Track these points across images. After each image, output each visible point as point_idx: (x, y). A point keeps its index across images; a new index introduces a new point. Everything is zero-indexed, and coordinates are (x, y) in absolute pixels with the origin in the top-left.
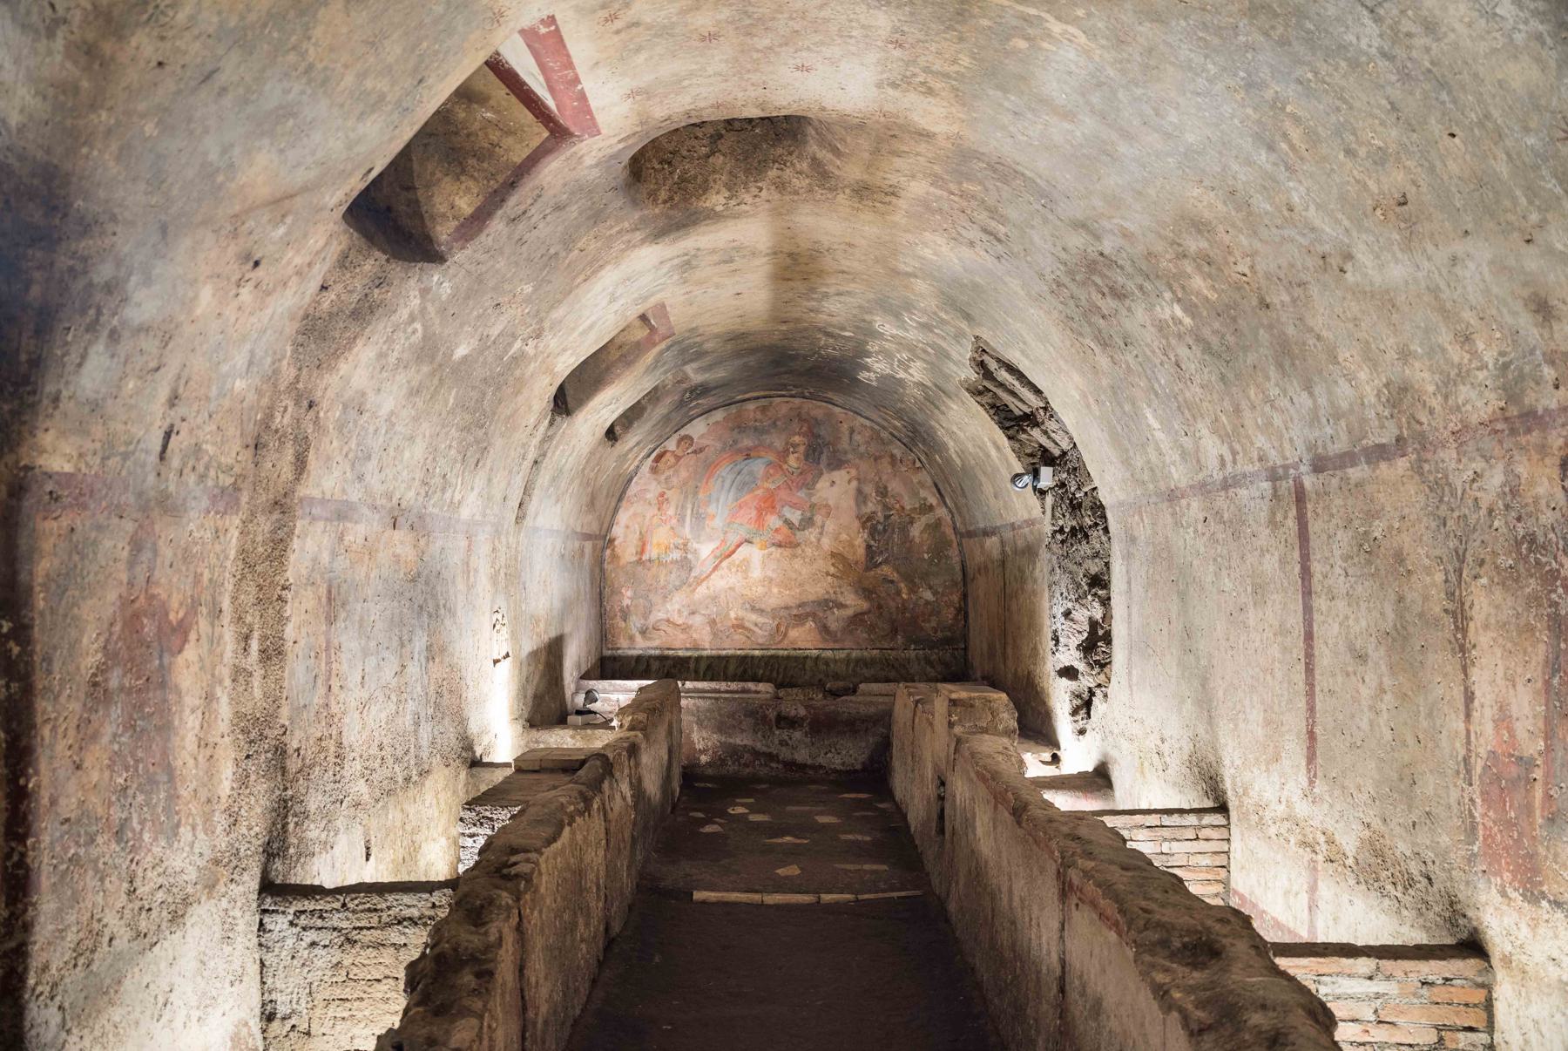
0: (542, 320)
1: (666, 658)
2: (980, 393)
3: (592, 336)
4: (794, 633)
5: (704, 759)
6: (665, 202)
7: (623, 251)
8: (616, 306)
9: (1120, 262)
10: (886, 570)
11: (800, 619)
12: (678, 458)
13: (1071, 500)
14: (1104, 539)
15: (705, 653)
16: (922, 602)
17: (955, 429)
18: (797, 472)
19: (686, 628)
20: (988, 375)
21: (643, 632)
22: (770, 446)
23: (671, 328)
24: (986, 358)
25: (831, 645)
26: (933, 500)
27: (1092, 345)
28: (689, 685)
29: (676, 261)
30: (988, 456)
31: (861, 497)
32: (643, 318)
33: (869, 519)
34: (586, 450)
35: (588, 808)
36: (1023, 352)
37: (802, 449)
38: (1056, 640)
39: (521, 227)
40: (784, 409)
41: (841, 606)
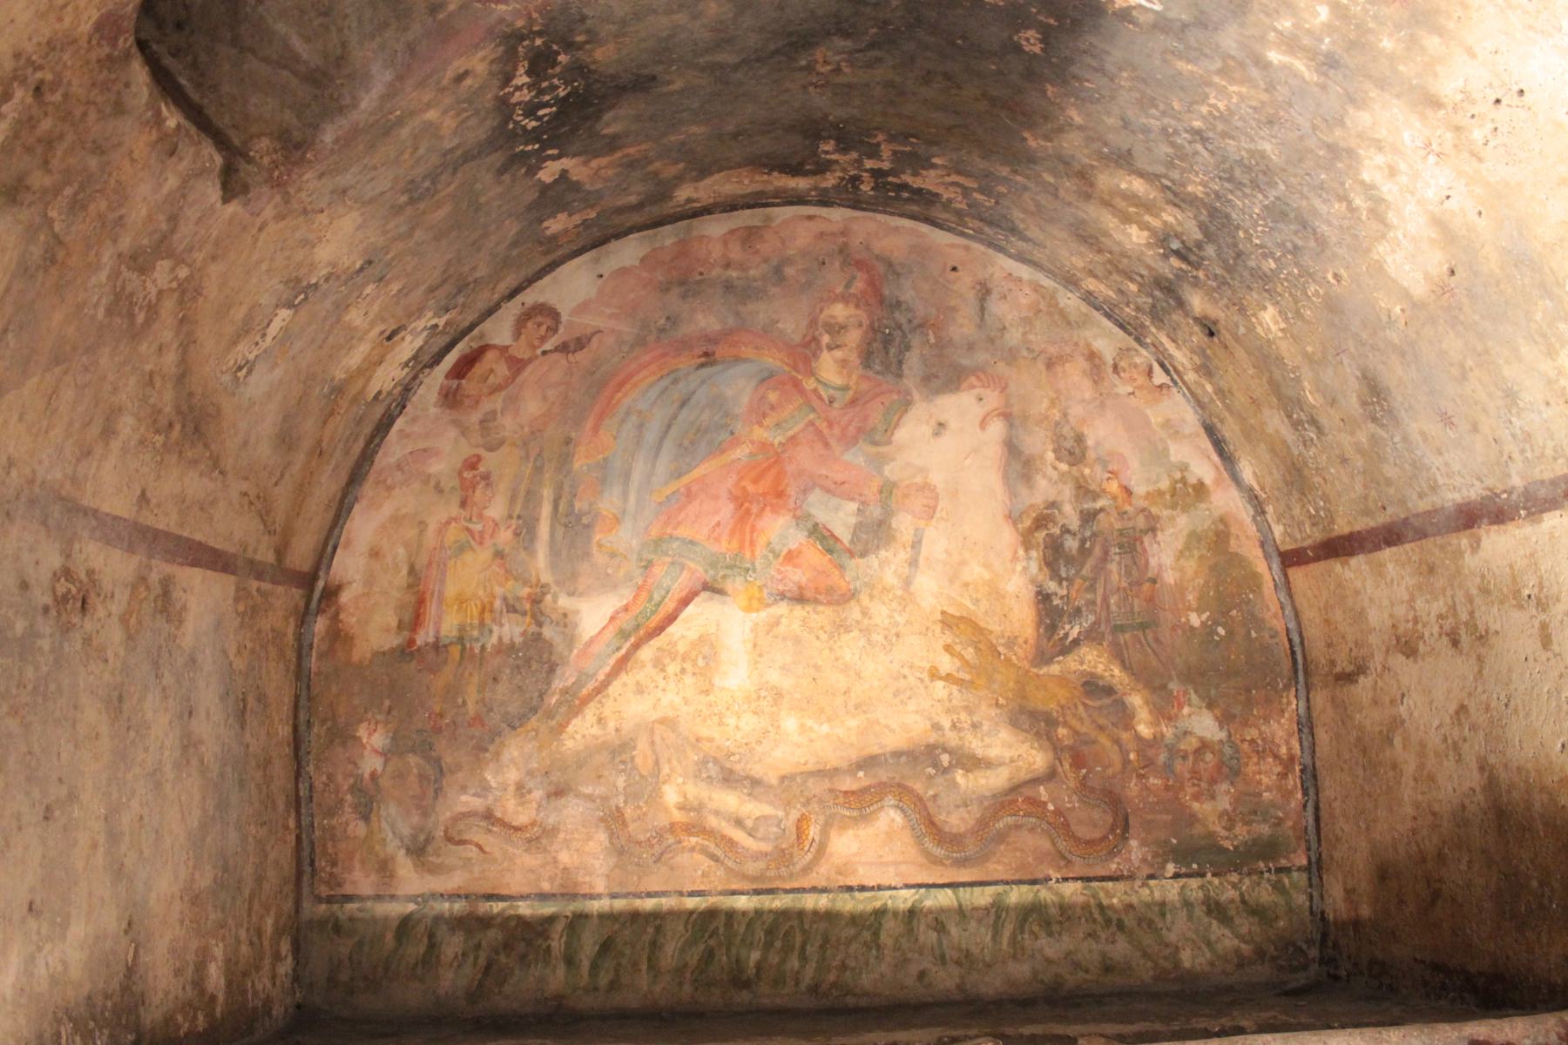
1: (486, 922)
10: (1092, 660)
11: (861, 803)
12: (517, 365)
15: (596, 906)
19: (538, 837)
21: (419, 850)
33: (1041, 522)
37: (854, 337)
41: (973, 763)
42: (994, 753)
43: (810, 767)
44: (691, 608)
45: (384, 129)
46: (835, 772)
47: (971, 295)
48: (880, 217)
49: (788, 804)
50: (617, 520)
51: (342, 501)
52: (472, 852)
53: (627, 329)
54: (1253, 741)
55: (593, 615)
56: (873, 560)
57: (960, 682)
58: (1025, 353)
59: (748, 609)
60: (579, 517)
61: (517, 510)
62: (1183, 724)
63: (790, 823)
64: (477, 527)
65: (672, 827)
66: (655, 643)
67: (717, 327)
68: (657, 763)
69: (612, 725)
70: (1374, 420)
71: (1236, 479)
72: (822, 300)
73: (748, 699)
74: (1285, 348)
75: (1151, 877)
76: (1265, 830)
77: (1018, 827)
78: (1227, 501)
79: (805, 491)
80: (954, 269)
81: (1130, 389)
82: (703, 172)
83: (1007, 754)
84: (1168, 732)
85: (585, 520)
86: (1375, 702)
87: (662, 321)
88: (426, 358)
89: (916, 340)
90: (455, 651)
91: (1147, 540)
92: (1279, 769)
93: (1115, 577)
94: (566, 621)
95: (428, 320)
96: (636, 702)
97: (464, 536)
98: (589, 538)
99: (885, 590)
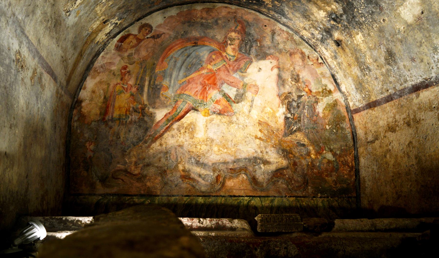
10: (299, 136)
12: (139, 41)
16: (325, 161)
18: (233, 59)
19: (141, 178)
21: (104, 180)
22: (213, 39)
25: (259, 194)
31: (281, 81)
33: (286, 97)
37: (237, 42)
40: (224, 13)
41: (266, 162)
42: (271, 160)
44: (188, 115)
48: (246, 9)
49: (214, 171)
50: (168, 88)
51: (84, 75)
52: (120, 182)
53: (172, 34)
54: (342, 161)
55: (160, 114)
56: (240, 104)
58: (284, 51)
59: (205, 116)
60: (156, 87)
61: (138, 82)
62: (324, 156)
64: (126, 87)
66: (178, 123)
67: (199, 36)
68: (177, 157)
69: (164, 146)
70: (389, 64)
71: (340, 90)
72: (228, 31)
73: (204, 141)
75: (314, 197)
79: (222, 84)
80: (266, 26)
81: (312, 63)
83: (276, 161)
85: (158, 87)
86: (380, 147)
87: (183, 32)
88: (112, 35)
89: (254, 45)
92: (349, 170)
93: (306, 114)
94: (152, 116)
96: (170, 140)
97: (121, 89)
98: (159, 92)
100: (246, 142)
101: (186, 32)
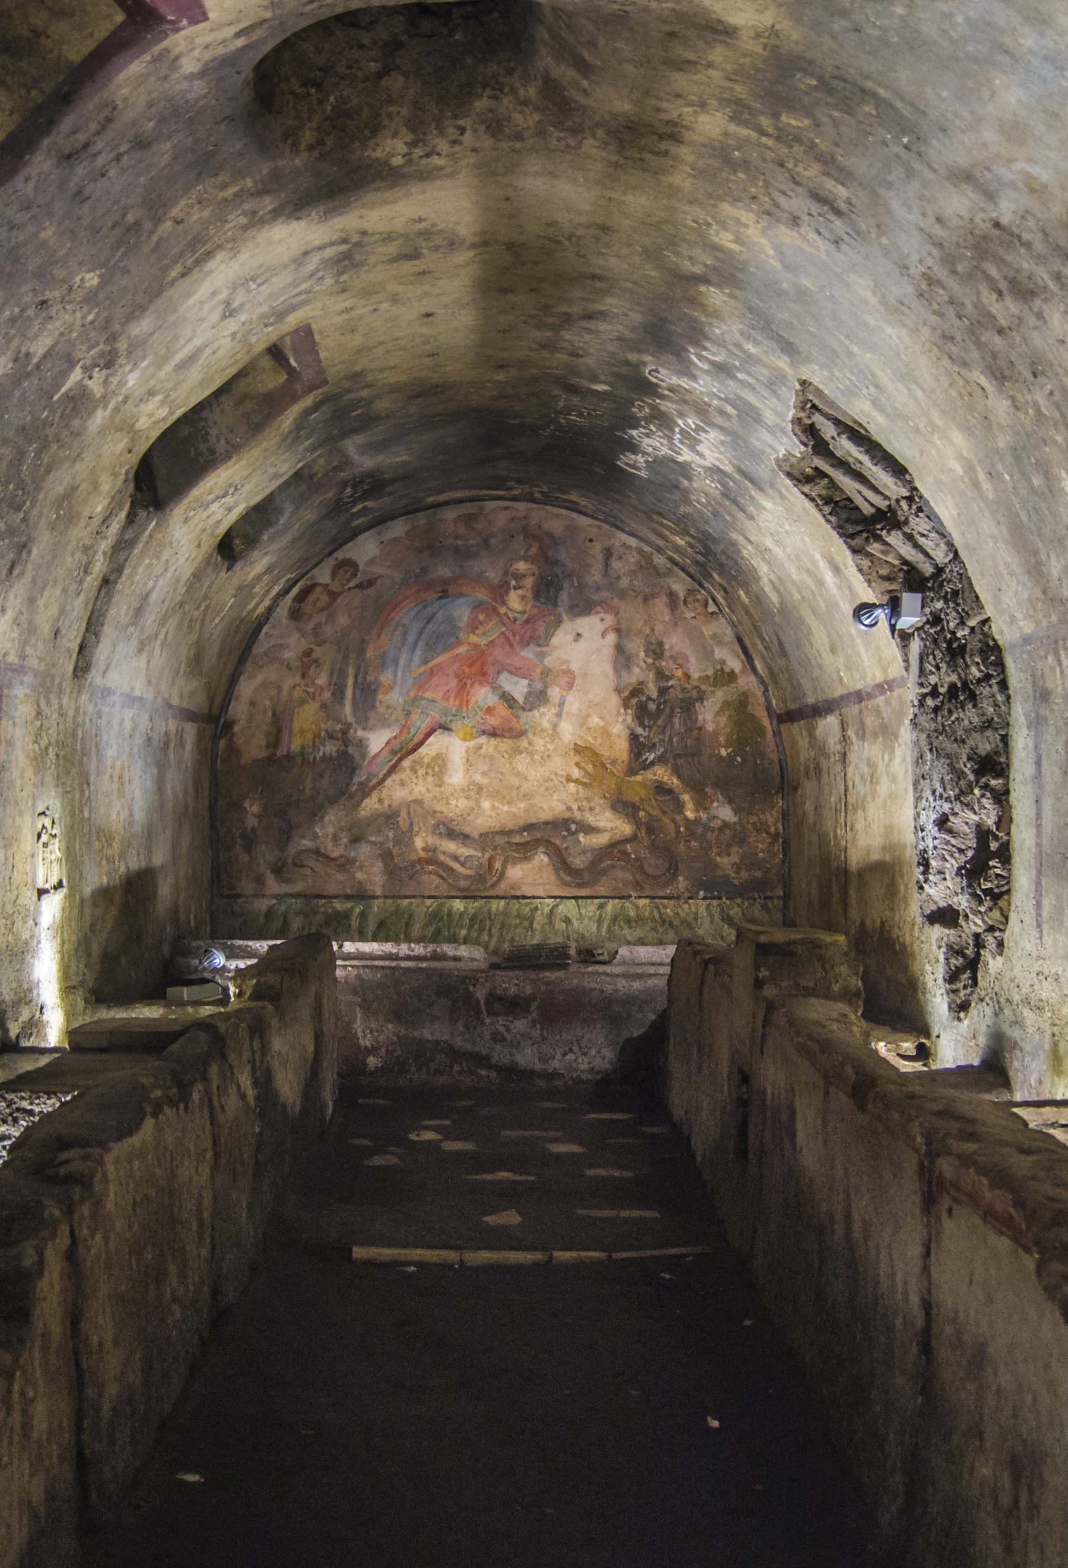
0: (113, 338)
2: (808, 480)
3: (195, 373)
4: (515, 873)
5: (373, 1061)
6: (311, 148)
7: (245, 228)
8: (232, 325)
9: (1026, 236)
10: (662, 774)
11: (525, 851)
12: (334, 595)
13: (949, 643)
14: (1000, 698)
17: (769, 543)
19: (345, 865)
20: (821, 447)
21: (278, 871)
22: (479, 579)
23: (321, 371)
24: (818, 419)
26: (735, 664)
27: (983, 381)
28: (349, 947)
29: (329, 253)
30: (821, 583)
31: (622, 657)
32: (275, 352)
33: (636, 692)
34: (187, 572)
35: (184, 1097)
36: (874, 402)
37: (529, 582)
38: (925, 864)
39: (81, 170)
40: (501, 520)
41: (589, 830)
42: (602, 824)
43: (497, 829)
44: (431, 739)
45: (287, 527)
46: (510, 833)
47: (600, 557)
49: (483, 850)
52: (308, 872)
55: (377, 741)
56: (536, 712)
57: (584, 784)
59: (464, 740)
61: (335, 680)
63: (485, 860)
64: (311, 690)
65: (420, 860)
68: (411, 825)
69: (386, 802)
73: (463, 790)
74: (751, 609)
75: (690, 898)
76: (758, 874)
77: (613, 867)
78: (747, 682)
79: (499, 673)
80: (591, 540)
82: (440, 492)
83: (609, 825)
84: (704, 816)
89: (566, 585)
90: (299, 760)
91: (697, 705)
93: (677, 726)
94: (361, 744)
95: (288, 576)
97: (305, 695)
98: (375, 696)
99: (543, 730)
100: (547, 789)
101: (424, 570)
